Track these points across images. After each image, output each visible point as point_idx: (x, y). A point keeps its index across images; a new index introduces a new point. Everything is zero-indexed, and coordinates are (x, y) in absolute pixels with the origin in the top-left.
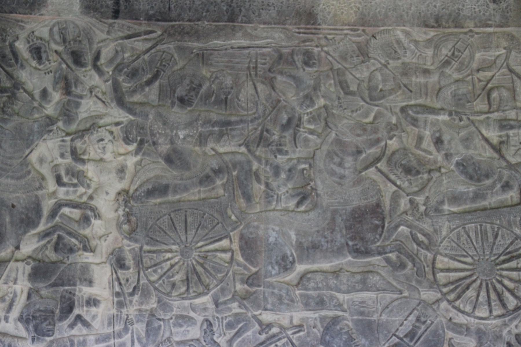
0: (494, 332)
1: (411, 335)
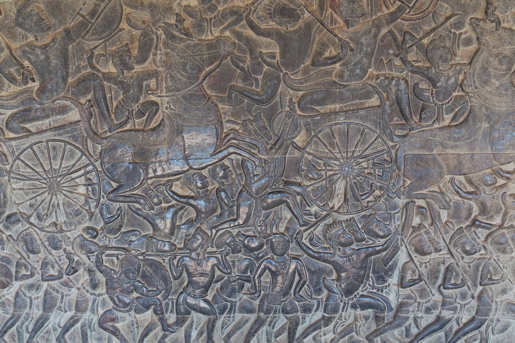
0: (164, 5)
1: (93, 13)
